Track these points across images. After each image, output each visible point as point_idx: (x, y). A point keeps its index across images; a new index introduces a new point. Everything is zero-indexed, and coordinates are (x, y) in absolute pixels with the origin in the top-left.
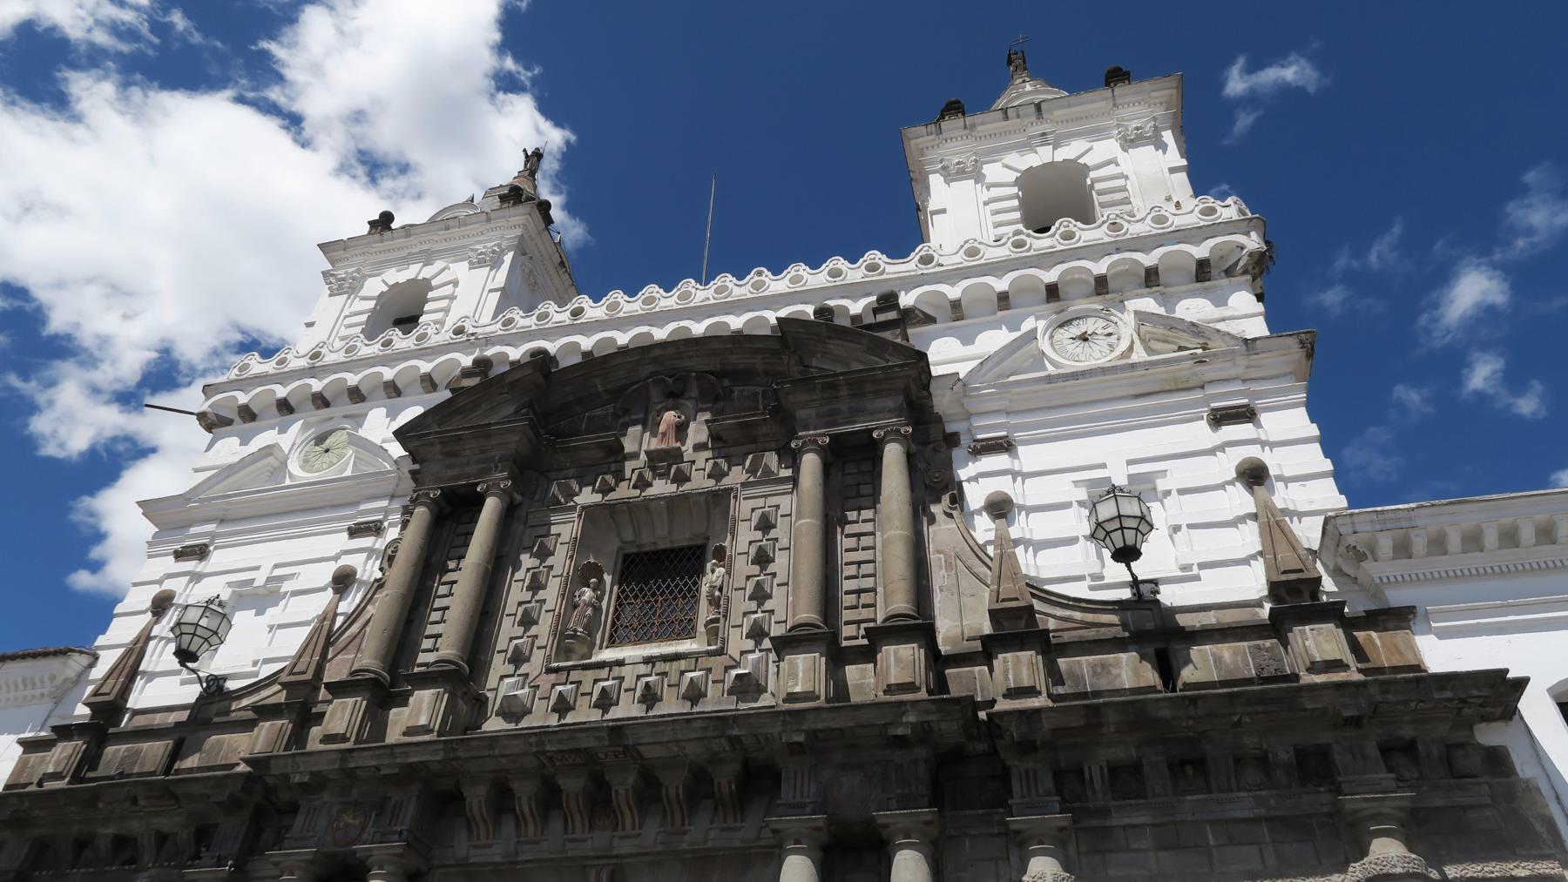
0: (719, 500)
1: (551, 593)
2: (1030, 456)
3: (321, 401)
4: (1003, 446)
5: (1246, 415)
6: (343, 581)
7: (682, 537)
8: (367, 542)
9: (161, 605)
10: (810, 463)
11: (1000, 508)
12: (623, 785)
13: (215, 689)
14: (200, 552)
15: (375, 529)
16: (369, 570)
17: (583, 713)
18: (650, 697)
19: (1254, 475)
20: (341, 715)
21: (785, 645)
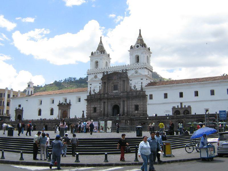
0: (118, 83)
1: (110, 88)
2: (133, 81)
3: (94, 73)
4: (131, 80)
5: (142, 79)
6: (100, 87)
7: (117, 84)
8: (100, 84)
9: (90, 88)
10: (122, 82)
11: (131, 84)
12: (115, 99)
13: (95, 93)
14: (91, 84)
15: (101, 83)
16: (101, 86)
17: (113, 95)
18: (116, 94)
19: (142, 83)
20: (102, 95)
21: (121, 93)
